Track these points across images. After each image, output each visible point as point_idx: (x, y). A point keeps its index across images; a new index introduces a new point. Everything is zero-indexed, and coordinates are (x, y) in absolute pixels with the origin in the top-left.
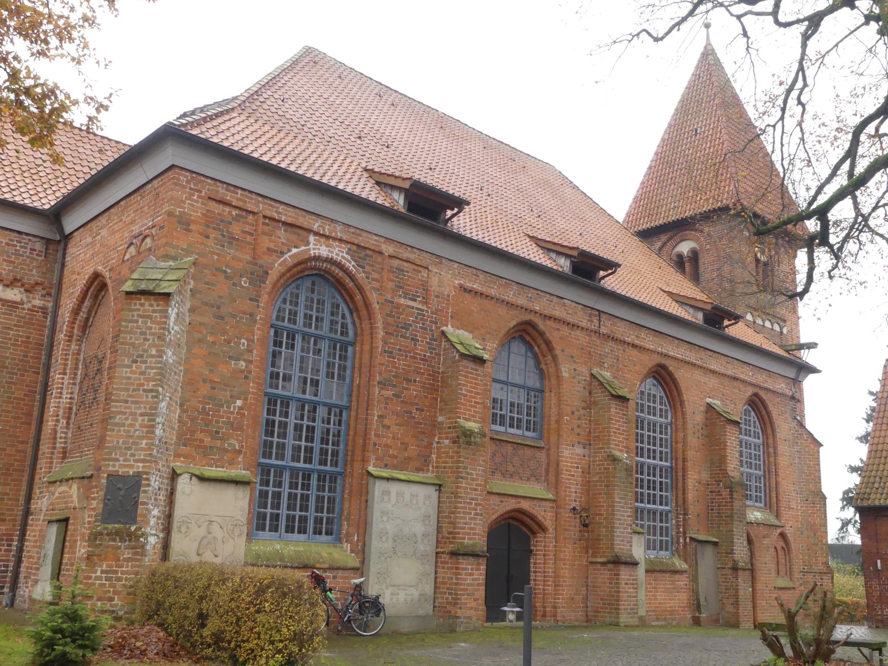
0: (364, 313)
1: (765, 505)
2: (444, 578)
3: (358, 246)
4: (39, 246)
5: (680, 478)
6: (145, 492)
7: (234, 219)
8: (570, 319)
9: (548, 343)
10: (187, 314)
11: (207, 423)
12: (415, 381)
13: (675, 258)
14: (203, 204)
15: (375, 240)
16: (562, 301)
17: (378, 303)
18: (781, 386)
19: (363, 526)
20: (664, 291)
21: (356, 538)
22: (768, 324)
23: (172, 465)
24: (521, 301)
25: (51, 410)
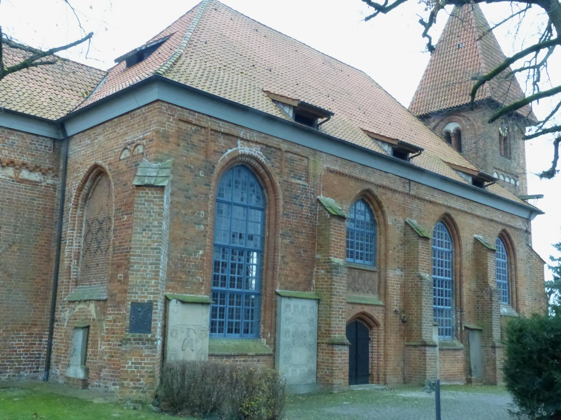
0: (271, 189)
1: (509, 303)
2: (323, 359)
3: (267, 146)
4: (50, 144)
5: (458, 288)
6: (156, 313)
7: (194, 132)
8: (393, 186)
9: (379, 203)
10: (170, 197)
11: (184, 267)
12: (302, 232)
13: (444, 134)
14: (176, 124)
15: (277, 141)
16: (387, 174)
17: (279, 183)
18: (519, 224)
19: (274, 328)
20: (445, 162)
21: (269, 335)
22: (507, 180)
23: (165, 293)
24: (363, 176)
25: (66, 254)
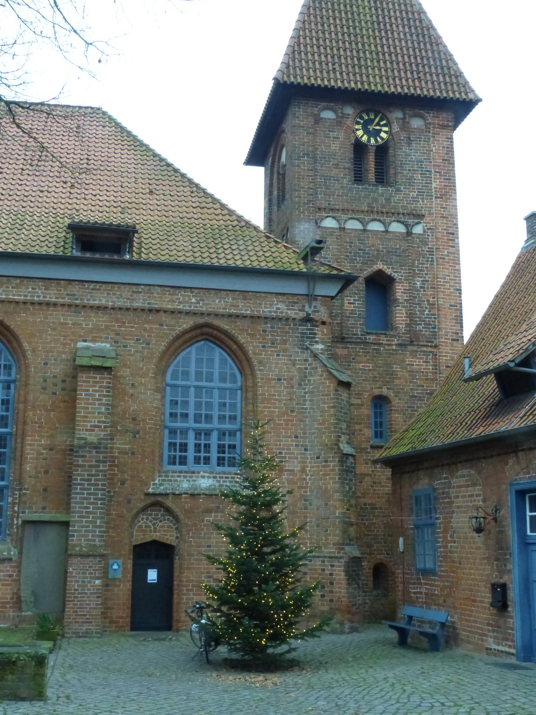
5: (19, 446)
